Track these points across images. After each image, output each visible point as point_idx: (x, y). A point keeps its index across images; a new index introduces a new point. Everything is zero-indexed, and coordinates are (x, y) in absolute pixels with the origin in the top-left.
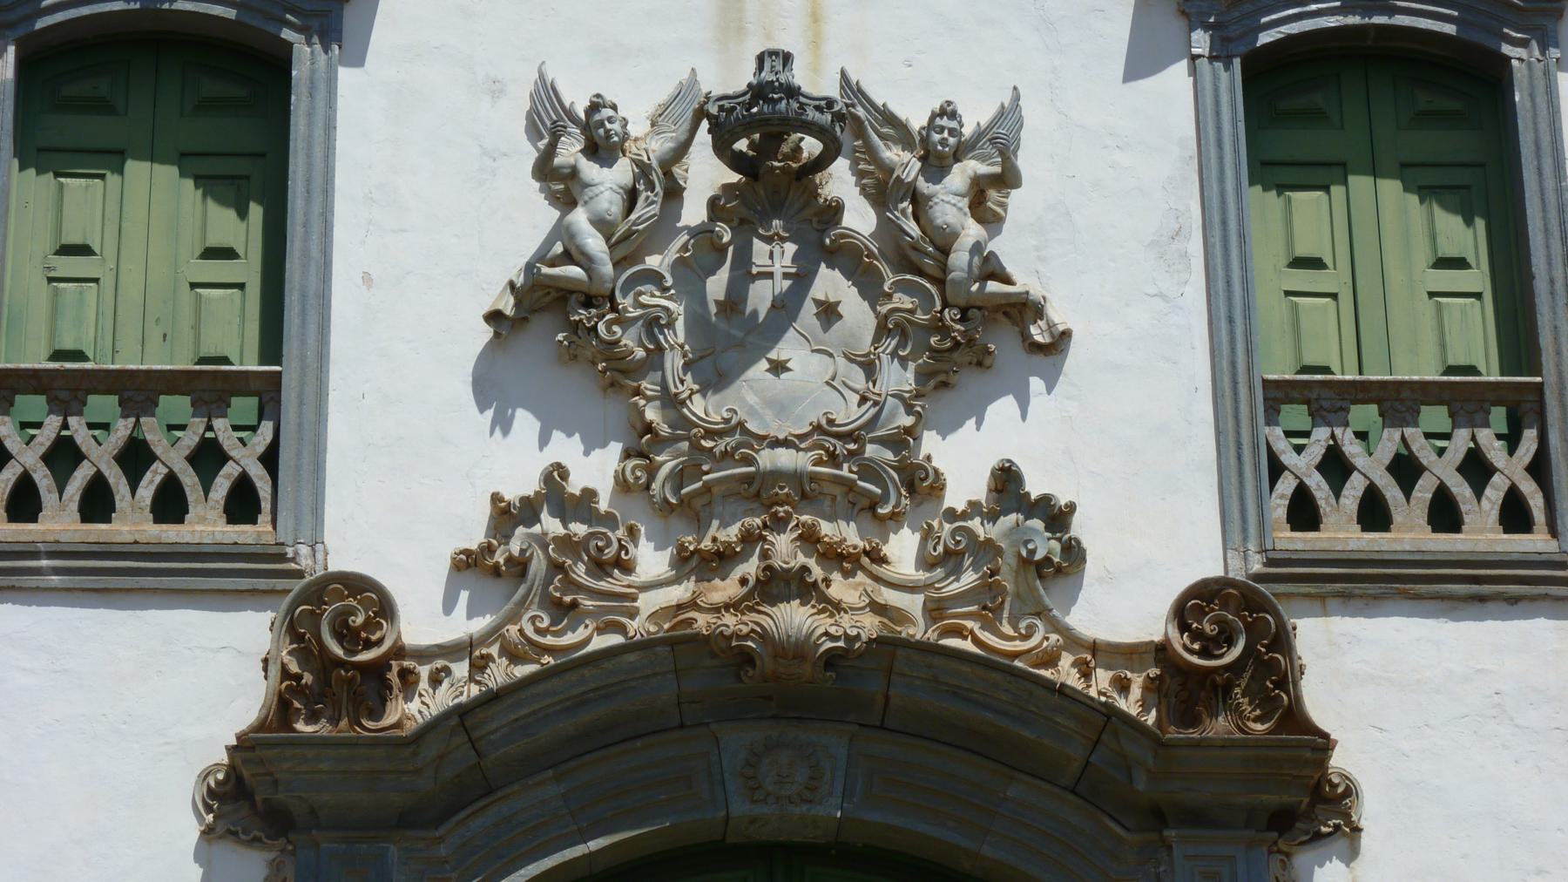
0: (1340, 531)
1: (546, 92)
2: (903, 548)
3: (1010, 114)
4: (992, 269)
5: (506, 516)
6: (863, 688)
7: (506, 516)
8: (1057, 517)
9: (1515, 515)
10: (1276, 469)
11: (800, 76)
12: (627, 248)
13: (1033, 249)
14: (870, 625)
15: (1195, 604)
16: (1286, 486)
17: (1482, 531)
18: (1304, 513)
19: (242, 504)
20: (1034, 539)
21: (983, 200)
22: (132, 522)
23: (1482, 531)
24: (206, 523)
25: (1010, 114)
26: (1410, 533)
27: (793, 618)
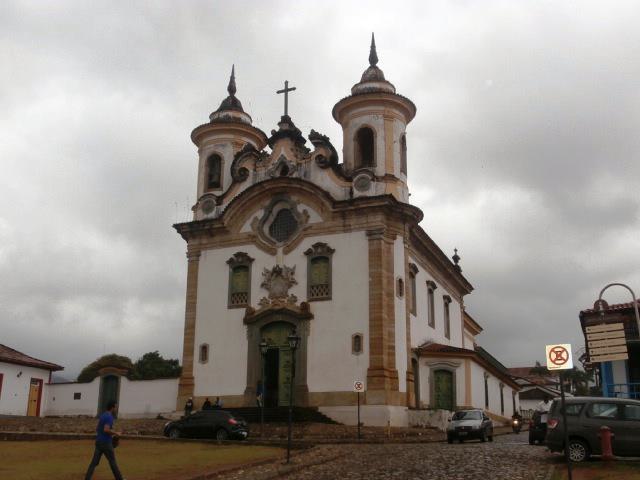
0: (315, 297)
2: (286, 301)
3: (294, 268)
6: (283, 311)
8: (295, 297)
12: (269, 280)
13: (295, 277)
14: (281, 307)
15: (303, 303)
17: (325, 296)
20: (294, 299)
21: (292, 274)
22: (240, 303)
23: (325, 296)
24: (244, 303)
25: (294, 268)
26: (320, 296)
27: (277, 308)
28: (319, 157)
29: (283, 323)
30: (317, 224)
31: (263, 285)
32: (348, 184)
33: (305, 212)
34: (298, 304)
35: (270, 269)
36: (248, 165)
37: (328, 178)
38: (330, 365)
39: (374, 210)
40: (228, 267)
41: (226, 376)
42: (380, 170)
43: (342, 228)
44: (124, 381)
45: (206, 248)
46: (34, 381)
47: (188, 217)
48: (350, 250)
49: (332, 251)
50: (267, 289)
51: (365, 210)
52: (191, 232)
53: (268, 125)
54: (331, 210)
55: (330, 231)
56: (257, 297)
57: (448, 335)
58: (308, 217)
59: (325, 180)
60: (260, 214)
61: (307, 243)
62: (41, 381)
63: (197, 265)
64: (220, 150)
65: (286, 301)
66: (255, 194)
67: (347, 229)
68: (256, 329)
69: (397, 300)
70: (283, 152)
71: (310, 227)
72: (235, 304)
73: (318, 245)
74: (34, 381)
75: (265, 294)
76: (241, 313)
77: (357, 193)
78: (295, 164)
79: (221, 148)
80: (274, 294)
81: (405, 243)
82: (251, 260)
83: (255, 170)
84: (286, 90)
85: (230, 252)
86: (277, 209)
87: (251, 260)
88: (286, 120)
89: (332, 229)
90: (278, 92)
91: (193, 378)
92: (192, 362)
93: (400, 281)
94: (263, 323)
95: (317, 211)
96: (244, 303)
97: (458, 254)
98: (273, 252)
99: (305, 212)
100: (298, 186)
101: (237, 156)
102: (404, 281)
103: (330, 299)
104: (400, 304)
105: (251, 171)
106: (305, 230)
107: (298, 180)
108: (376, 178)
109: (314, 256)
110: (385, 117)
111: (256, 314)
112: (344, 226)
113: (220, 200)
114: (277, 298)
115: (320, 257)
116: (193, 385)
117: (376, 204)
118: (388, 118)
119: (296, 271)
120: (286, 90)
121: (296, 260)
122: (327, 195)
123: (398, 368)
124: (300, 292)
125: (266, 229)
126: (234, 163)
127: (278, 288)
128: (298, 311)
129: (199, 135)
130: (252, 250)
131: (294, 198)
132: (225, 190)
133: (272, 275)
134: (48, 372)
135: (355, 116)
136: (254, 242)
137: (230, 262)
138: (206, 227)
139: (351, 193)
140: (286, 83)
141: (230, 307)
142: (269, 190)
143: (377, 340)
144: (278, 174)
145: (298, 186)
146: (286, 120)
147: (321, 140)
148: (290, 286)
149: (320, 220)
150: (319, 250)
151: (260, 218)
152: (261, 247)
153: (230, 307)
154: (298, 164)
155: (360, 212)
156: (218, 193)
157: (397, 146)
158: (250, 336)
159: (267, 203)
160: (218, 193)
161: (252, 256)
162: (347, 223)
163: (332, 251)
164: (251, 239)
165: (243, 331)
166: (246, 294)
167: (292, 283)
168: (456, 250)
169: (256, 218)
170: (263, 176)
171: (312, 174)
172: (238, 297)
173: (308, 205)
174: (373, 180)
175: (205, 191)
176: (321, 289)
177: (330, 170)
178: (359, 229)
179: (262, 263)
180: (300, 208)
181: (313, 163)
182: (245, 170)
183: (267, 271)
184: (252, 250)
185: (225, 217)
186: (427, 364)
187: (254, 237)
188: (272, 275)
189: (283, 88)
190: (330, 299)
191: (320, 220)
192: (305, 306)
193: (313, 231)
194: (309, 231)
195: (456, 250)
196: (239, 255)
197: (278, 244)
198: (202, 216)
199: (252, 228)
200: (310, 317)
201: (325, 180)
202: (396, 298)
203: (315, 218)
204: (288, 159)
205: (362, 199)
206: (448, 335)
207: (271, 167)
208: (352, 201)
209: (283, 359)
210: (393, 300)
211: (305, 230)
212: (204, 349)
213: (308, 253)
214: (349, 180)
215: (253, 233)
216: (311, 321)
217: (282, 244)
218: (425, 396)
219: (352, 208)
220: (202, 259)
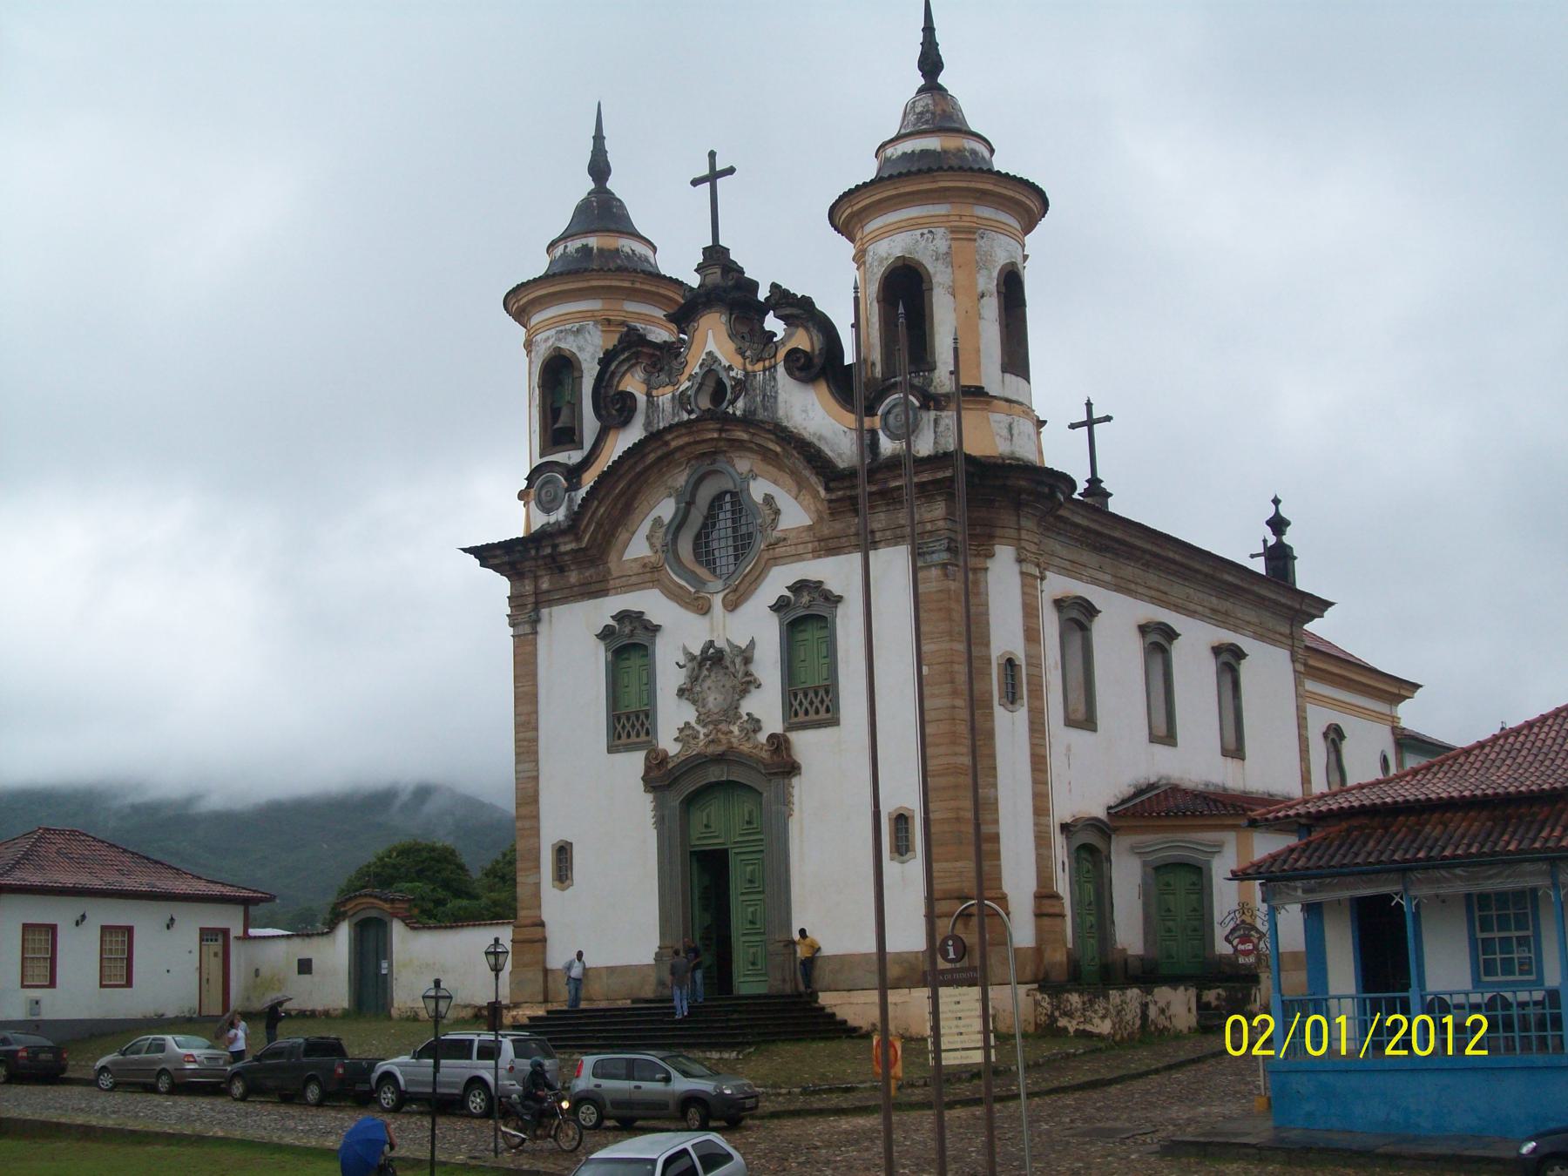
0: (802, 718)
1: (685, 648)
2: (735, 729)
3: (752, 642)
4: (747, 674)
5: (681, 730)
7: (681, 730)
8: (758, 721)
9: (828, 710)
12: (694, 679)
14: (720, 749)
17: (823, 715)
18: (796, 714)
19: (648, 733)
20: (755, 724)
21: (747, 661)
22: (633, 739)
23: (823, 715)
24: (643, 737)
25: (752, 642)
26: (812, 716)
28: (793, 353)
29: (729, 787)
31: (681, 692)
33: (769, 499)
34: (762, 737)
35: (697, 651)
36: (633, 384)
37: (818, 405)
38: (842, 891)
39: (926, 491)
40: (601, 647)
41: (610, 917)
42: (942, 379)
43: (853, 540)
44: (398, 930)
45: (551, 603)
46: (206, 935)
47: (510, 521)
48: (880, 592)
50: (694, 702)
53: (680, 262)
54: (822, 493)
55: (828, 547)
56: (673, 719)
57: (1235, 749)
58: (777, 512)
59: (811, 412)
60: (666, 509)
61: (777, 582)
62: (225, 933)
63: (535, 644)
64: (569, 345)
65: (735, 729)
67: (867, 543)
68: (674, 800)
69: (1001, 714)
70: (711, 346)
72: (624, 740)
73: (799, 587)
74: (206, 935)
75: (688, 713)
76: (635, 762)
77: (887, 446)
79: (571, 338)
80: (708, 714)
81: (1020, 561)
82: (655, 629)
84: (713, 176)
85: (604, 610)
88: (716, 256)
89: (832, 544)
91: (542, 924)
92: (538, 885)
93: (1010, 663)
94: (689, 786)
95: (789, 491)
96: (643, 737)
97: (1284, 513)
98: (704, 609)
99: (769, 499)
101: (606, 360)
102: (1021, 658)
103: (834, 722)
104: (1010, 727)
105: (641, 399)
106: (772, 546)
107: (747, 421)
108: (932, 401)
109: (793, 615)
110: (954, 230)
111: (670, 766)
113: (574, 474)
114: (716, 723)
115: (806, 616)
116: (544, 940)
118: (965, 233)
119: (758, 654)
120: (713, 176)
121: (755, 626)
123: (1008, 887)
124: (766, 706)
125: (685, 548)
127: (714, 700)
128: (765, 755)
129: (521, 302)
130: (652, 604)
131: (743, 464)
132: (588, 446)
133: (701, 665)
134: (241, 908)
135: (876, 238)
136: (656, 583)
137: (606, 634)
140: (712, 155)
141: (612, 749)
142: (681, 448)
143: (952, 825)
144: (705, 403)
145: (745, 436)
146: (716, 256)
147: (799, 310)
148: (744, 692)
150: (805, 599)
151: (666, 520)
153: (612, 749)
154: (747, 374)
155: (889, 498)
156: (573, 457)
157: (991, 308)
158: (660, 822)
159: (681, 479)
160: (573, 457)
164: (649, 575)
165: (644, 803)
166: (647, 717)
167: (749, 684)
168: (1276, 502)
169: (658, 521)
170: (668, 407)
171: (782, 397)
172: (628, 722)
173: (775, 482)
174: (925, 406)
175: (542, 456)
176: (812, 701)
177: (823, 387)
178: (896, 540)
179: (680, 632)
180: (758, 489)
181: (781, 369)
183: (692, 658)
184: (652, 604)
186: (1135, 850)
187: (655, 569)
188: (701, 665)
189: (706, 171)
190: (834, 722)
192: (779, 744)
193: (792, 550)
194: (780, 551)
195: (1276, 502)
196: (622, 617)
198: (540, 520)
199: (652, 545)
200: (792, 769)
201: (811, 412)
202: (999, 712)
203: (795, 514)
205: (894, 463)
206: (1235, 749)
207: (687, 384)
208: (878, 467)
209: (738, 874)
210: (990, 716)
211: (772, 546)
212: (563, 852)
213: (780, 606)
216: (795, 781)
217: (719, 584)
218: (1129, 935)
220: (542, 628)
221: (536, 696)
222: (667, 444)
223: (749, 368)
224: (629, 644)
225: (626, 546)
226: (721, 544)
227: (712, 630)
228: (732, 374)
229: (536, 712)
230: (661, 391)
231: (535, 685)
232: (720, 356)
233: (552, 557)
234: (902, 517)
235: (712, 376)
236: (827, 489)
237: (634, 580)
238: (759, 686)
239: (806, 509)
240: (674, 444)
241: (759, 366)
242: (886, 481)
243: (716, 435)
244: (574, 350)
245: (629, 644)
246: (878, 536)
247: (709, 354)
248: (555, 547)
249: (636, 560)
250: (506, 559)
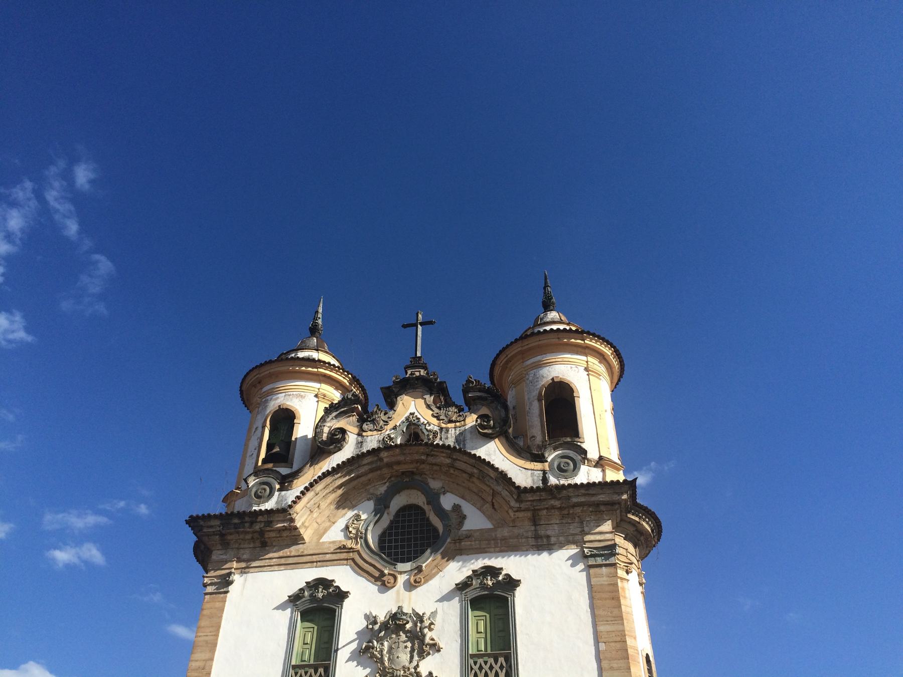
10: (472, 669)
11: (405, 611)
16: (473, 672)
30: (481, 531)
32: (539, 466)
33: (457, 508)
35: (381, 618)
43: (532, 542)
49: (512, 584)
51: (578, 510)
52: (222, 535)
58: (464, 517)
64: (293, 403)
66: (362, 470)
70: (412, 409)
71: (469, 536)
78: (436, 429)
82: (341, 596)
83: (359, 435)
85: (297, 579)
86: (398, 502)
87: (341, 596)
89: (513, 541)
90: (405, 326)
95: (474, 505)
99: (457, 508)
100: (448, 461)
112: (537, 537)
113: (286, 482)
117: (602, 498)
122: (503, 477)
126: (323, 420)
130: (342, 576)
132: (295, 467)
138: (257, 527)
139: (545, 480)
142: (389, 465)
149: (488, 525)
152: (360, 569)
154: (441, 429)
156: (284, 471)
159: (382, 489)
160: (284, 471)
161: (344, 589)
162: (542, 533)
163: (512, 584)
173: (463, 497)
179: (363, 603)
180: (448, 501)
182: (343, 431)
184: (342, 576)
185: (298, 507)
191: (488, 525)
197: (401, 566)
203: (476, 521)
204: (422, 420)
213: (462, 587)
214: (541, 459)
215: (349, 544)
217: (407, 566)
219: (557, 503)
221: (215, 645)
222: (381, 460)
223: (443, 425)
224: (319, 607)
225: (326, 530)
226: (406, 541)
227: (398, 600)
228: (428, 428)
229: (212, 659)
230: (369, 433)
231: (217, 635)
232: (419, 416)
233: (262, 533)
234: (574, 528)
235: (413, 428)
236: (519, 500)
237: (328, 557)
238: (439, 651)
239: (489, 518)
240: (385, 460)
241: (449, 425)
242: (569, 497)
243: (423, 457)
244: (297, 407)
245: (319, 607)
246: (553, 540)
247: (412, 414)
248: (269, 523)
249: (334, 542)
250: (218, 529)
